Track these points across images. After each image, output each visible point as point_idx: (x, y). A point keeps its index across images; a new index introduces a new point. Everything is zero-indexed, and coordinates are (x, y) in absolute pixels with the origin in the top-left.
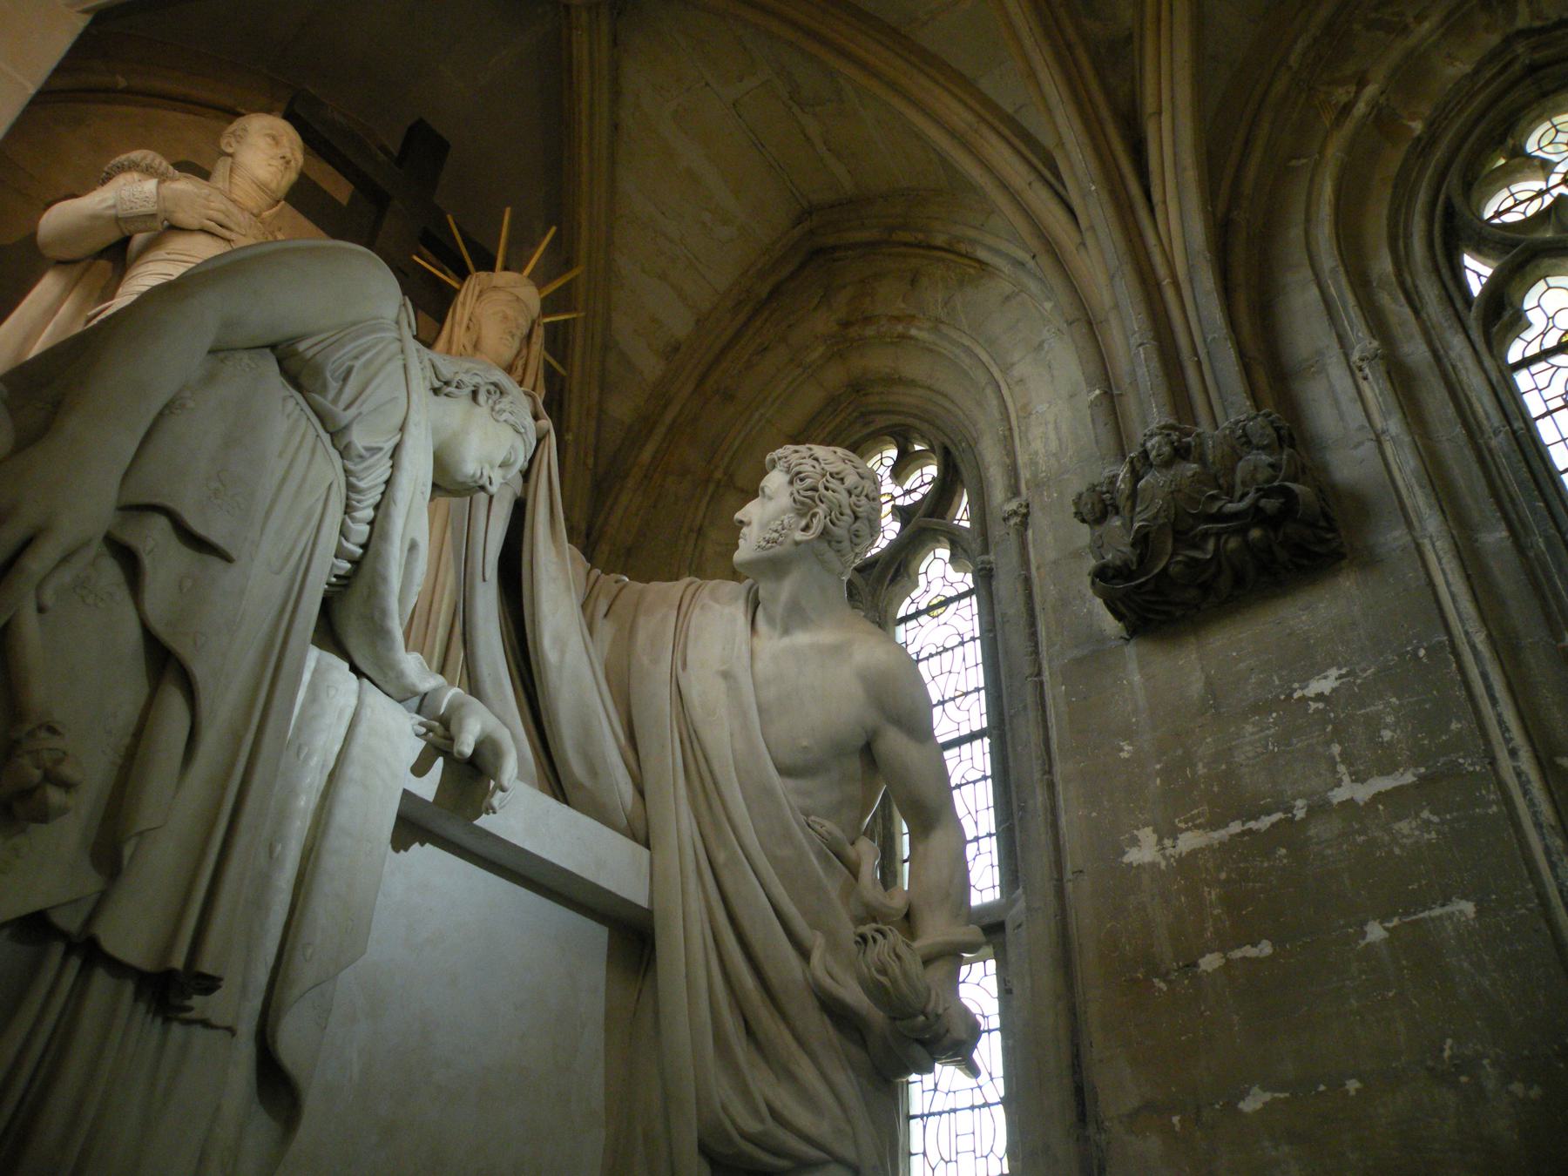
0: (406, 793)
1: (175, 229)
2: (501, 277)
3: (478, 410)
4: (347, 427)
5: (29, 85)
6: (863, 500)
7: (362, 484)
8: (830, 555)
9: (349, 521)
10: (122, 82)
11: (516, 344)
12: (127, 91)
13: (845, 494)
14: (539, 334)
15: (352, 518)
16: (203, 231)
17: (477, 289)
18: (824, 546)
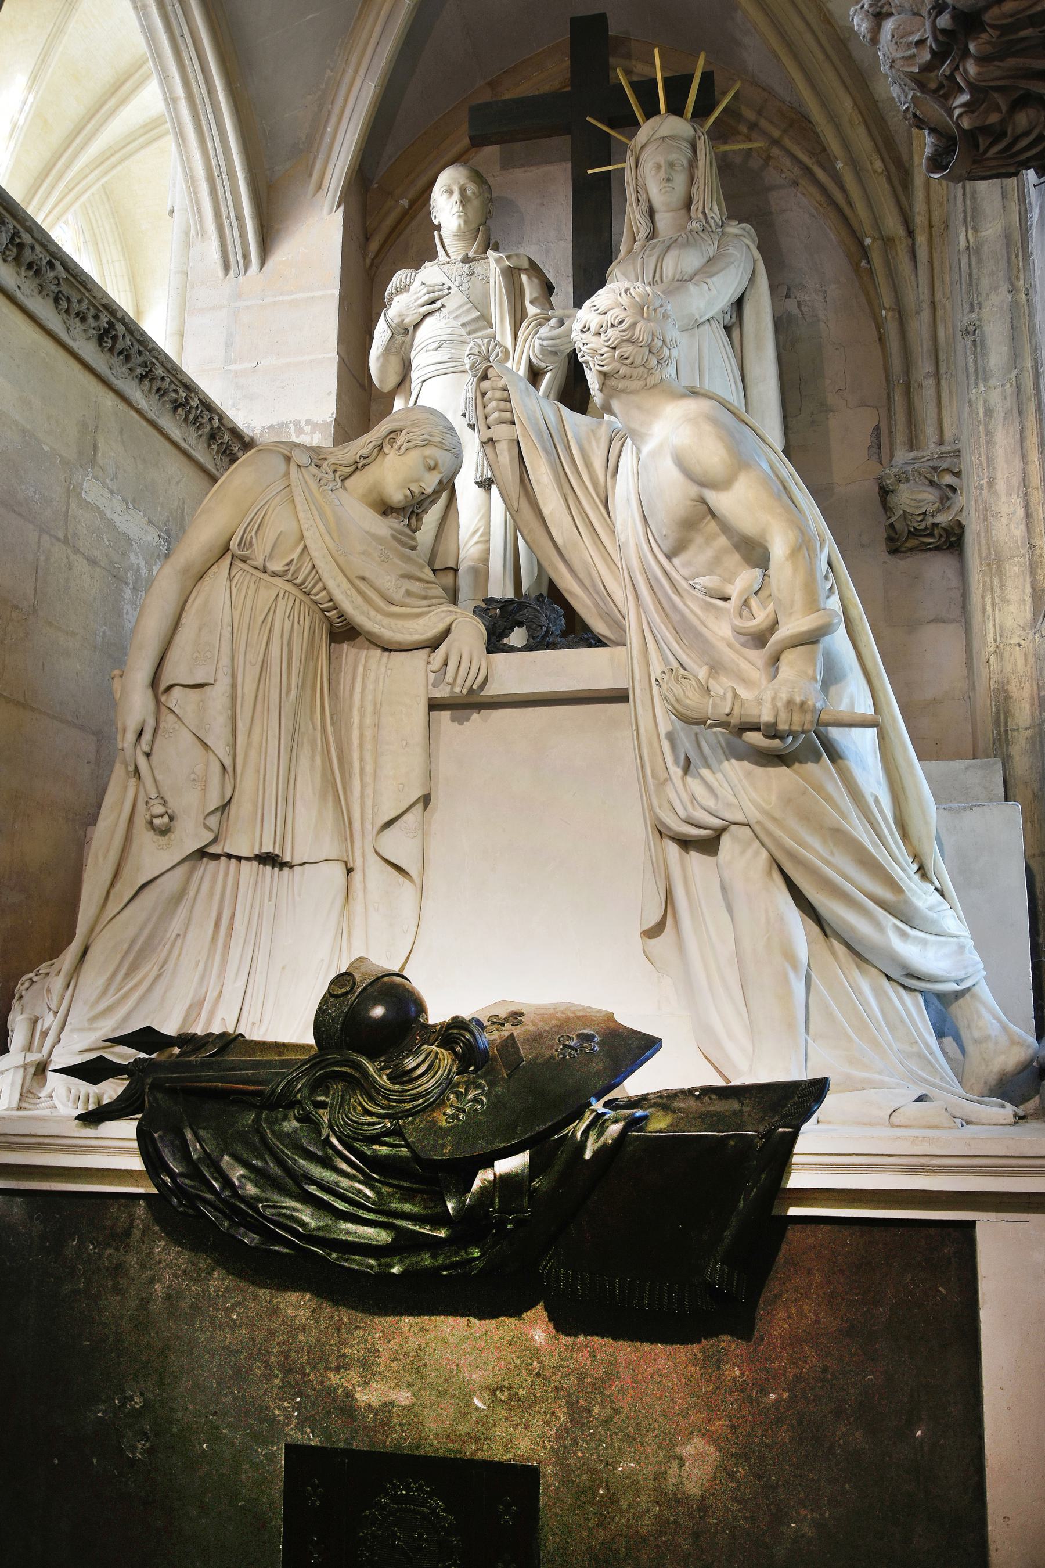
0: (430, 700)
1: (416, 326)
2: (646, 130)
3: (388, 457)
4: (264, 567)
5: (329, 292)
6: (610, 331)
7: (298, 581)
8: (622, 384)
9: (313, 597)
10: (405, 203)
11: (680, 180)
12: (411, 206)
13: (595, 339)
14: (702, 144)
15: (316, 595)
16: (425, 316)
17: (633, 159)
18: (613, 382)
